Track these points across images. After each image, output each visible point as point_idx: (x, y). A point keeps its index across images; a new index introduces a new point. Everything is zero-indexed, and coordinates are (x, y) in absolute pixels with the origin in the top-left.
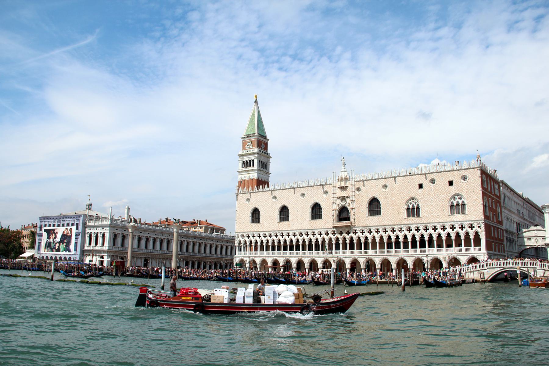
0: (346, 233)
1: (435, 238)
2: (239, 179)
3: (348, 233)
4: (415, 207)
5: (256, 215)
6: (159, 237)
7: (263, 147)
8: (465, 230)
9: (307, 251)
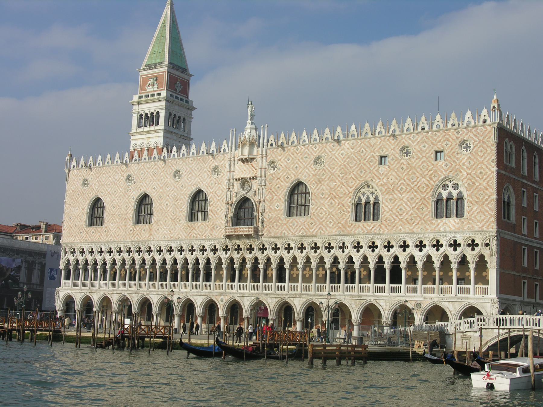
2: (132, 149)
3: (250, 249)
4: (372, 202)
5: (96, 212)
7: (179, 89)
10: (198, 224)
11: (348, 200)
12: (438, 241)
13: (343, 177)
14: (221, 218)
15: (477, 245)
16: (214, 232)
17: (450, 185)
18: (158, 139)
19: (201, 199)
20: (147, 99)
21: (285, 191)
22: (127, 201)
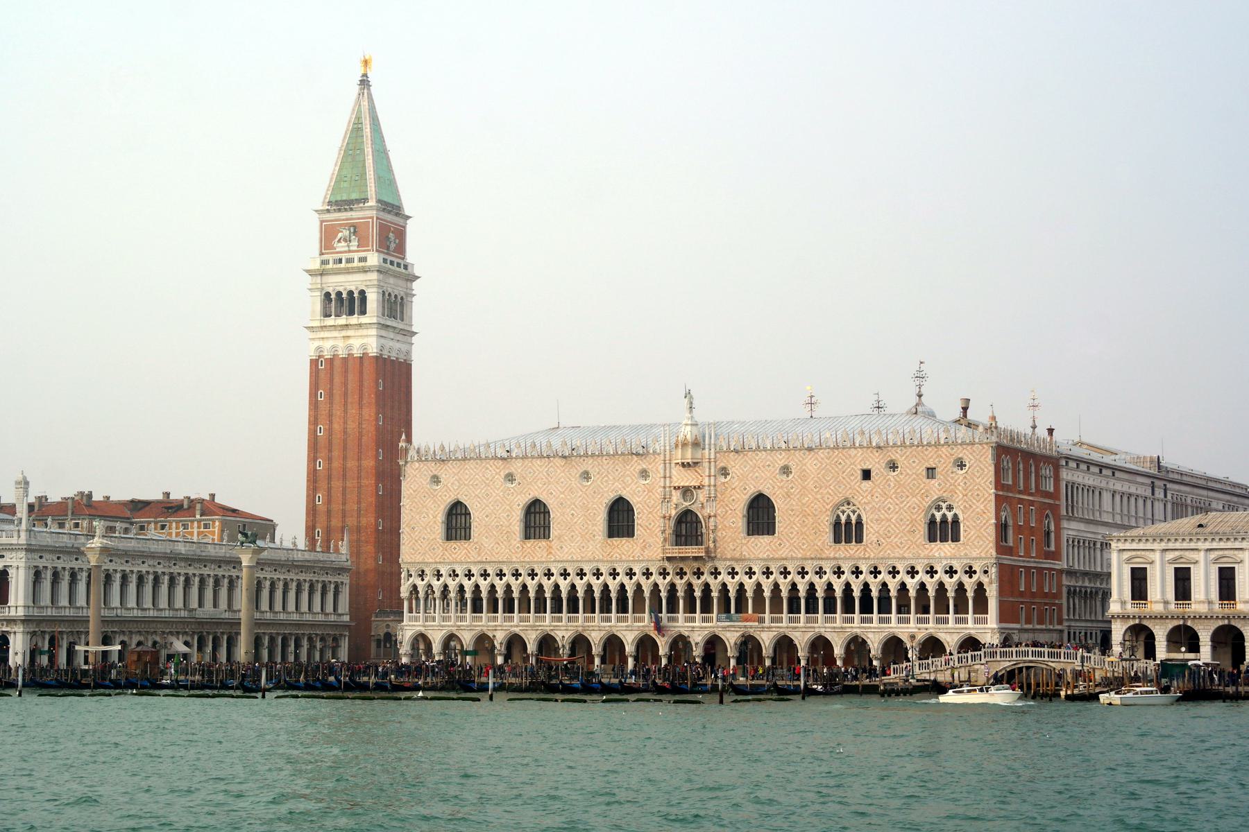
0: (694, 573)
1: (893, 593)
2: (312, 354)
3: (699, 574)
4: (854, 522)
5: (457, 521)
6: (135, 570)
7: (393, 246)
8: (956, 577)
9: (597, 615)
10: (622, 543)
12: (932, 567)
15: (975, 572)
17: (944, 505)
18: (365, 341)
20: (339, 266)
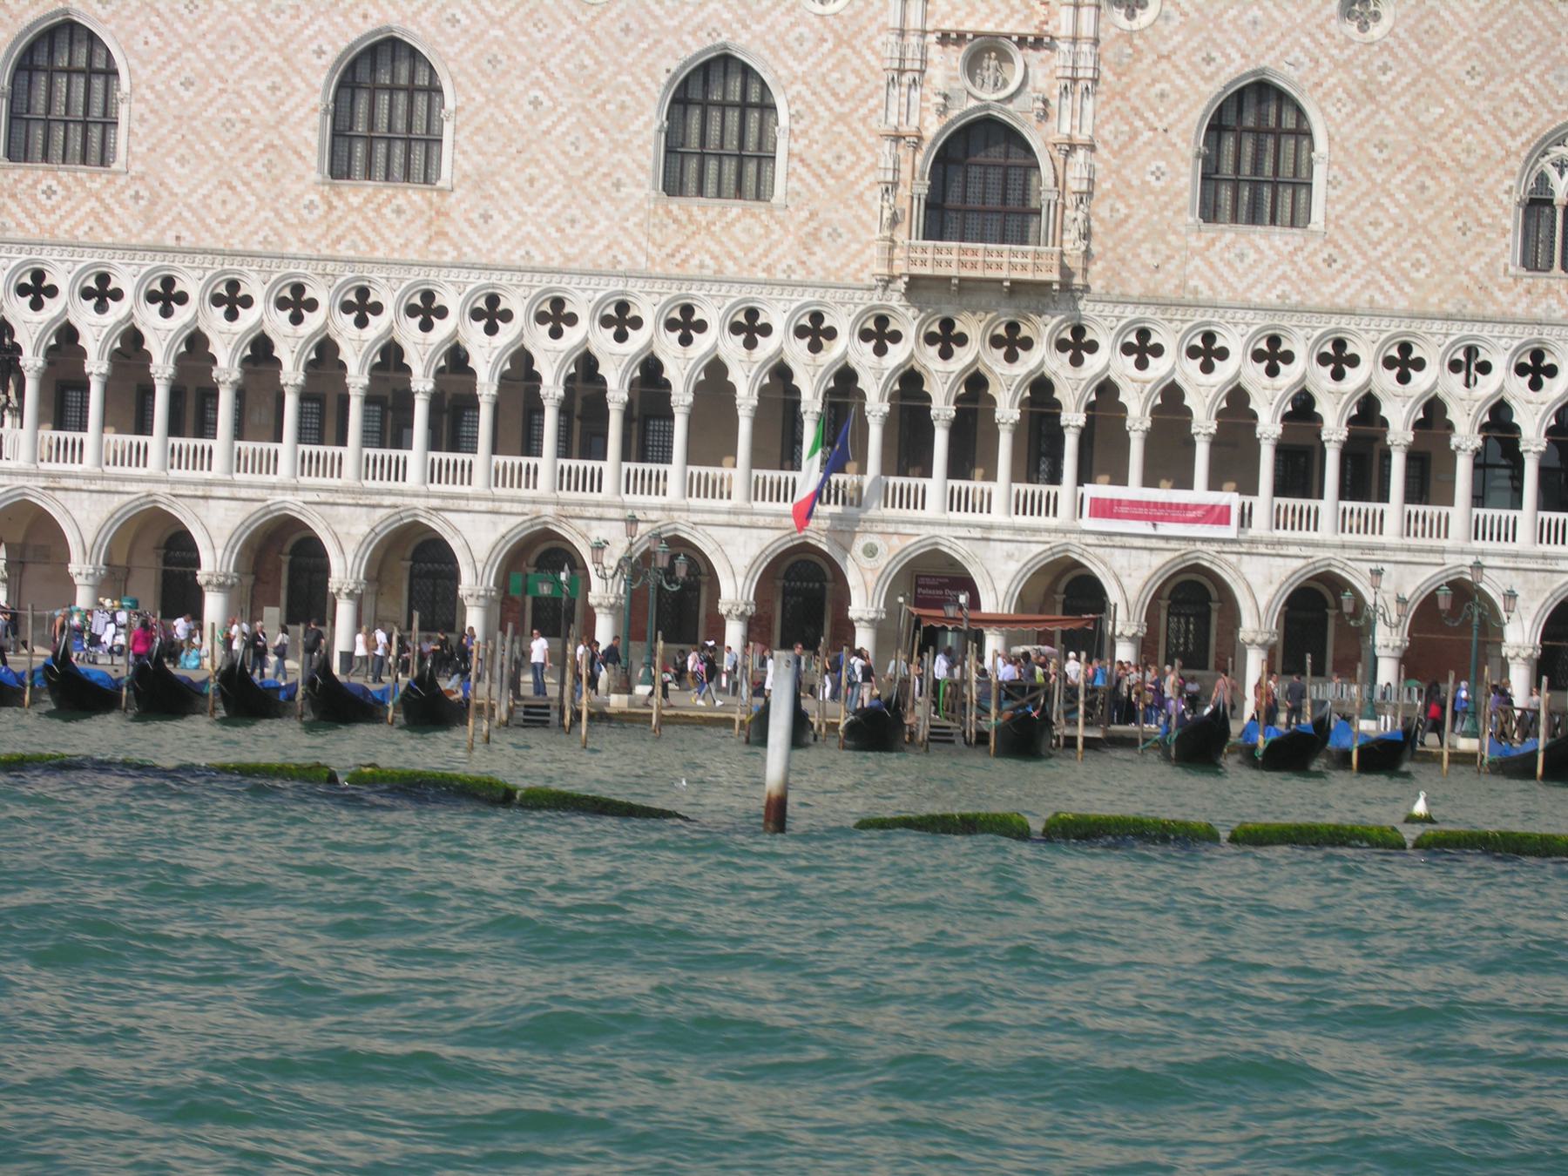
3: (1012, 343)
11: (1499, 182)
13: (1481, 88)
14: (860, 197)
16: (820, 254)
19: (716, 96)
21: (1197, 114)
22: (275, 58)
